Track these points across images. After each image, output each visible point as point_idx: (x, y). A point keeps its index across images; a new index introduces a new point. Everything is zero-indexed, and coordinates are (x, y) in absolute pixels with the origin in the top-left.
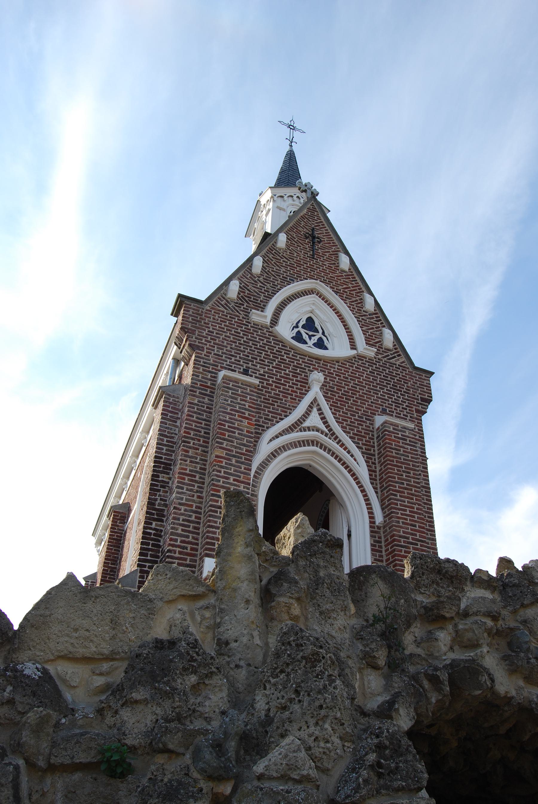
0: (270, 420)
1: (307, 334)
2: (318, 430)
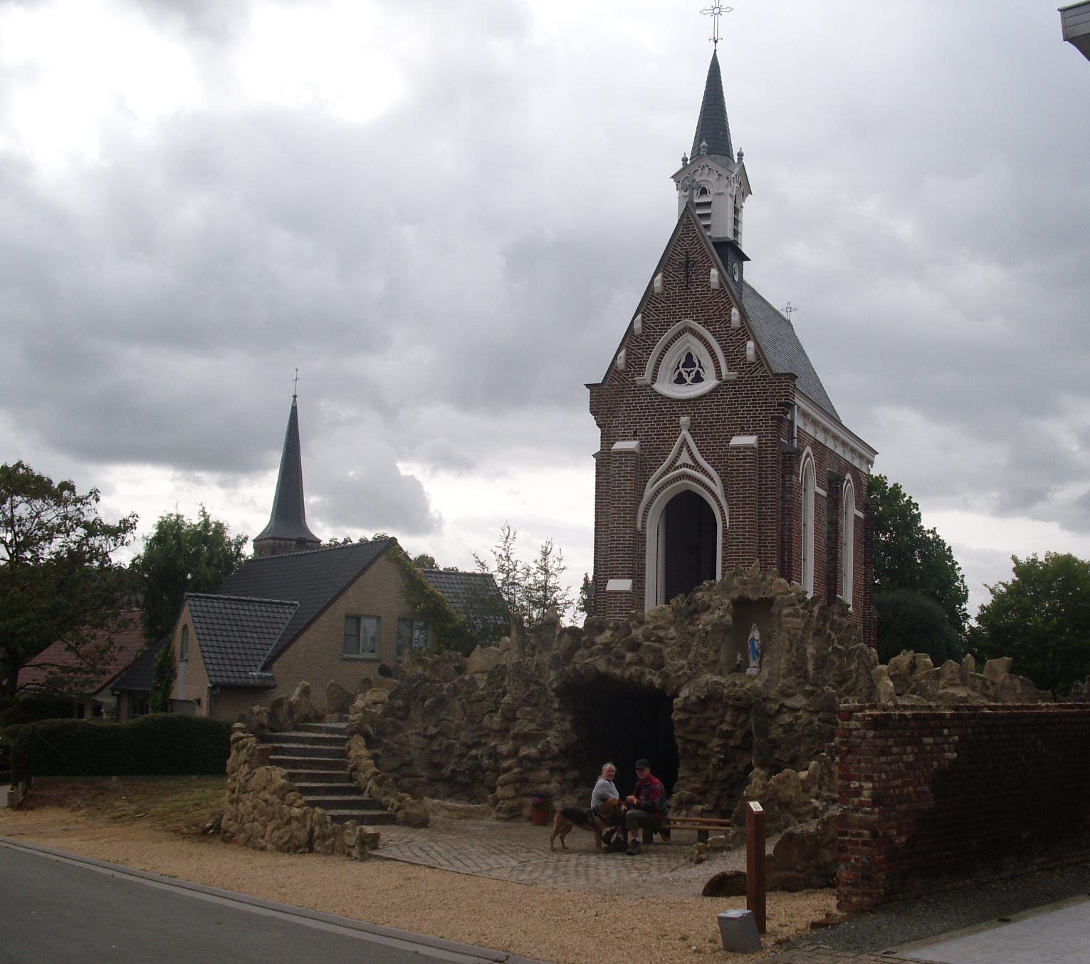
0: (653, 468)
1: (686, 371)
2: (687, 466)
